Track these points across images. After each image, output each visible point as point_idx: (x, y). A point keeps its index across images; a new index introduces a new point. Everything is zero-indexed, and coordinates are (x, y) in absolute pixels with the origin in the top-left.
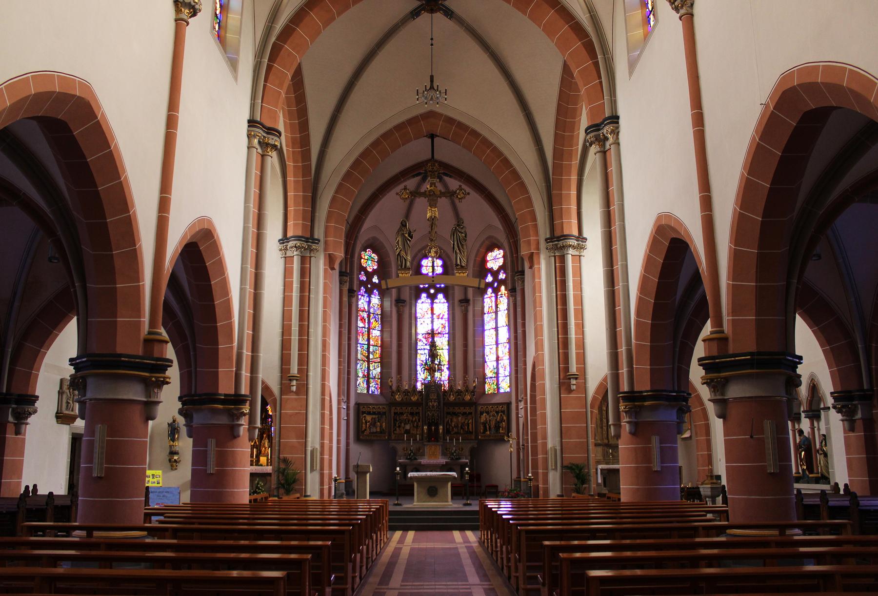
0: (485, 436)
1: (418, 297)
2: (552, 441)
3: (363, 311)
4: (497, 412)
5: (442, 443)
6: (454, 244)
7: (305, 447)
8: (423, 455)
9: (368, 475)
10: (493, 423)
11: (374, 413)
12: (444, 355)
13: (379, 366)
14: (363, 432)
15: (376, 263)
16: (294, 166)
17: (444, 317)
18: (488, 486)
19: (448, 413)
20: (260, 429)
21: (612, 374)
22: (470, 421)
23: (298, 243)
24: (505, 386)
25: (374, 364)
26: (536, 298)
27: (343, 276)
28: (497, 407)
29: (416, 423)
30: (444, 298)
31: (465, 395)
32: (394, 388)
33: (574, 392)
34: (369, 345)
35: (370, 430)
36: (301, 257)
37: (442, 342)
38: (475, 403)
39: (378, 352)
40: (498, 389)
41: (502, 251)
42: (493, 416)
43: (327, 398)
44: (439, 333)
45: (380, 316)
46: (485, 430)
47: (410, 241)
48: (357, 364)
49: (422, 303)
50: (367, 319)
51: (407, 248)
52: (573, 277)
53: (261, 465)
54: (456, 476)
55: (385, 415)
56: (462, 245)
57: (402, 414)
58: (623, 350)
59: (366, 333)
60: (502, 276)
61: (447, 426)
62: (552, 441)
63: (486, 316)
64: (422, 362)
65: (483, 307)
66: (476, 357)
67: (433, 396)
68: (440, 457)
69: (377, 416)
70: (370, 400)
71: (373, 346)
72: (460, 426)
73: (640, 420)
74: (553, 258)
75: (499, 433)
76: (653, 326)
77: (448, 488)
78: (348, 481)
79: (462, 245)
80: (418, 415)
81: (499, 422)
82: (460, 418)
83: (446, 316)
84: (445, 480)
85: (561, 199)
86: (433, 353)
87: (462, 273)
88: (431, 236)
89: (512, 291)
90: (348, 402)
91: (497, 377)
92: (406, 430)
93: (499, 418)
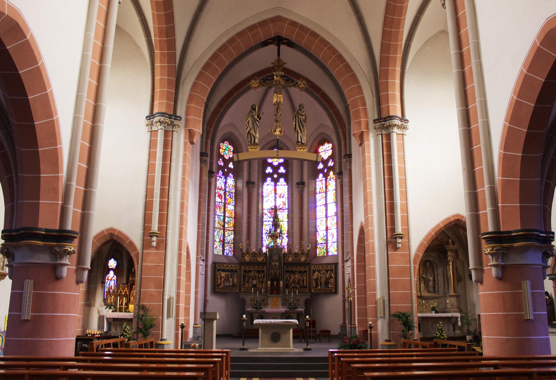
0: (317, 290)
1: (264, 180)
2: (380, 293)
3: (220, 189)
4: (327, 271)
5: (282, 295)
6: (296, 125)
7: (163, 296)
8: (266, 305)
9: (215, 322)
10: (323, 280)
11: (228, 271)
12: (284, 226)
13: (233, 233)
14: (218, 286)
15: (232, 153)
16: (161, 53)
17: (284, 196)
18: (322, 331)
19: (287, 272)
20: (90, 271)
21: (472, 216)
22: (305, 278)
23: (162, 119)
24: (333, 250)
25: (228, 231)
26: (365, 169)
27: (203, 156)
28: (327, 267)
29: (261, 279)
30: (284, 181)
31: (301, 257)
32: (244, 250)
33: (399, 249)
34: (224, 216)
35: (224, 284)
36: (165, 131)
37: (283, 216)
38: (310, 263)
39: (232, 222)
40: (327, 252)
41: (331, 145)
42: (323, 273)
43: (184, 253)
44: (280, 209)
45: (234, 194)
46: (317, 285)
47: (258, 121)
48: (214, 231)
49: (268, 185)
50: (223, 196)
51: (256, 127)
52: (398, 152)
53: (129, 312)
54: (298, 323)
55: (237, 272)
56: (303, 126)
57: (250, 271)
58: (485, 189)
59: (223, 207)
60: (331, 164)
61: (286, 282)
62: (380, 293)
63: (317, 195)
64: (266, 231)
65: (315, 188)
66: (310, 227)
67: (276, 258)
68: (281, 307)
69: (230, 273)
70: (225, 261)
71: (228, 217)
72: (296, 282)
73: (506, 263)
74: (380, 136)
75: (328, 287)
76: (524, 159)
77: (290, 335)
78: (196, 327)
79: (303, 126)
80: (263, 272)
81: (328, 279)
82: (297, 276)
83: (286, 196)
84: (287, 327)
85: (387, 85)
86: (276, 224)
87: (302, 148)
88: (276, 118)
89: (339, 175)
90: (206, 260)
91: (327, 243)
92: (254, 285)
93: (328, 275)
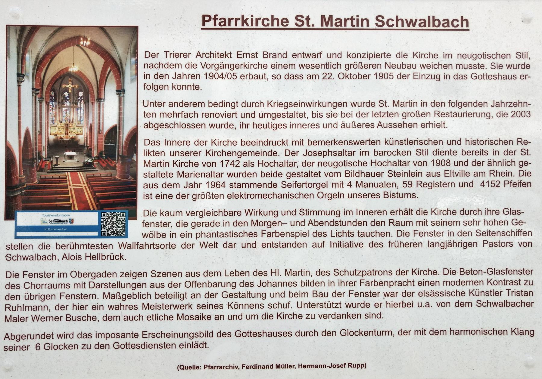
60: (82, 98)
89: (85, 103)
